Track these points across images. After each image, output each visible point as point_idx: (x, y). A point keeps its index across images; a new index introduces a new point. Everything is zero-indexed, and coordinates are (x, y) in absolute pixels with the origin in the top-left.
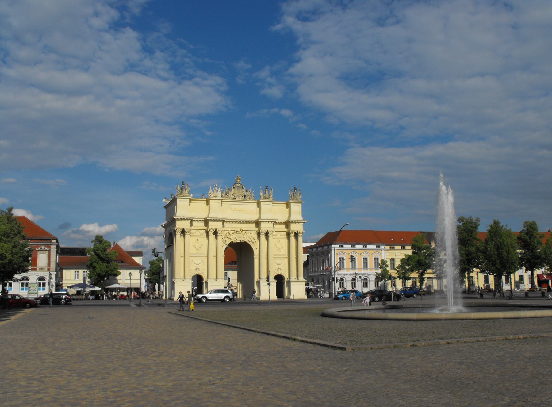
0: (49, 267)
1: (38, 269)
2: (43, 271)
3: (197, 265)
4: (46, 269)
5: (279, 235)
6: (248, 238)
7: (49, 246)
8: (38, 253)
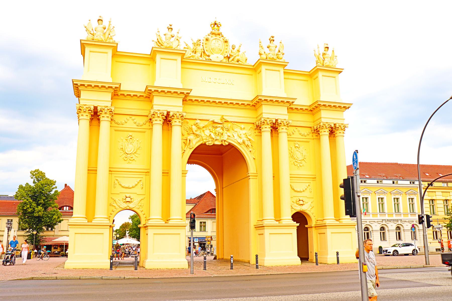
5: (297, 135)
6: (236, 137)
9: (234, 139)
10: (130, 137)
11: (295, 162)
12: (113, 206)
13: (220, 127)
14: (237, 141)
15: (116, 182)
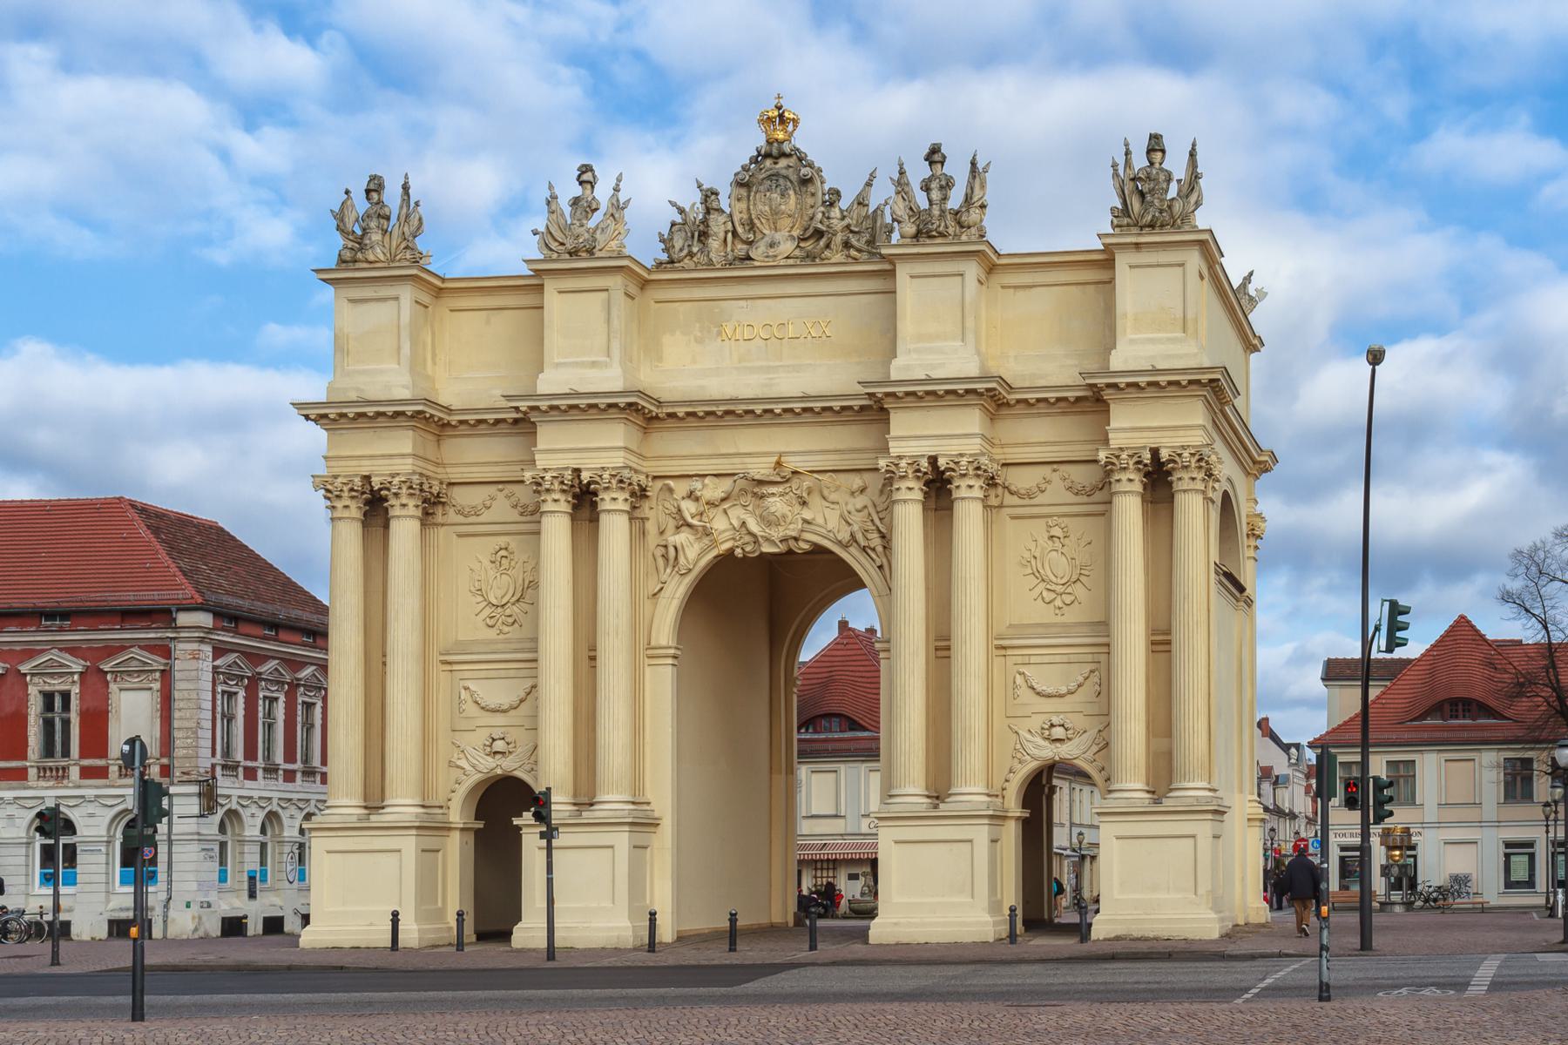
3: (499, 719)
6: (833, 521)
9: (824, 531)
11: (1045, 594)
12: (458, 767)
13: (773, 494)
14: (831, 535)
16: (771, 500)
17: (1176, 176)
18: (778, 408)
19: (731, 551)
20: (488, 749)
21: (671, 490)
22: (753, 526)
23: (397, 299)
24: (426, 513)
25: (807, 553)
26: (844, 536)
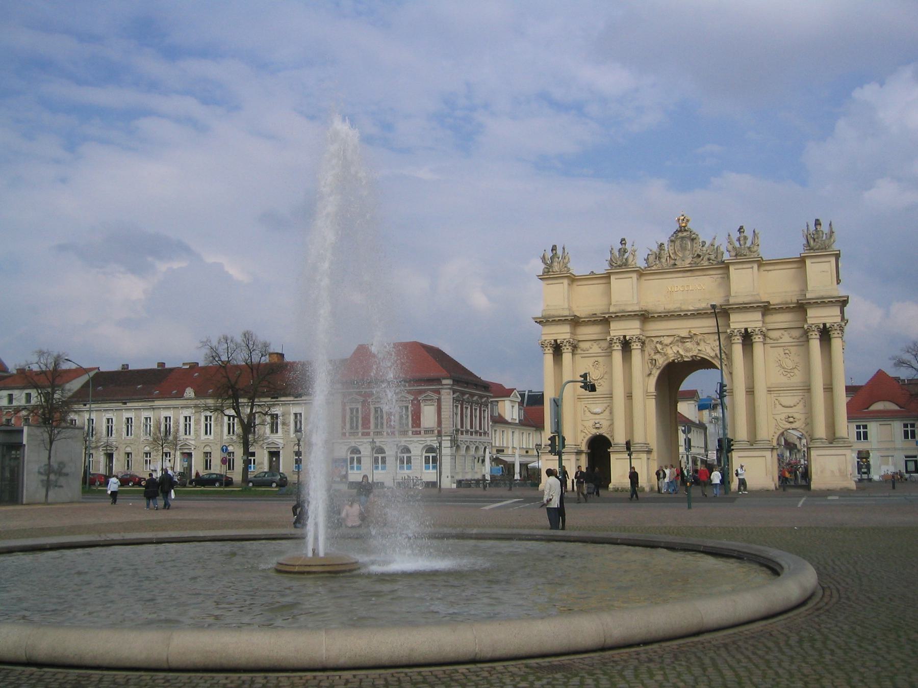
0: (439, 429)
1: (422, 432)
2: (431, 435)
4: (436, 432)
7: (438, 392)
8: (422, 405)
10: (596, 363)
11: (784, 372)
15: (586, 409)
16: (688, 343)
17: (825, 233)
18: (689, 313)
19: (674, 360)
20: (594, 427)
21: (653, 341)
22: (682, 352)
23: (563, 283)
24: (573, 351)
25: (699, 361)
26: (713, 354)
